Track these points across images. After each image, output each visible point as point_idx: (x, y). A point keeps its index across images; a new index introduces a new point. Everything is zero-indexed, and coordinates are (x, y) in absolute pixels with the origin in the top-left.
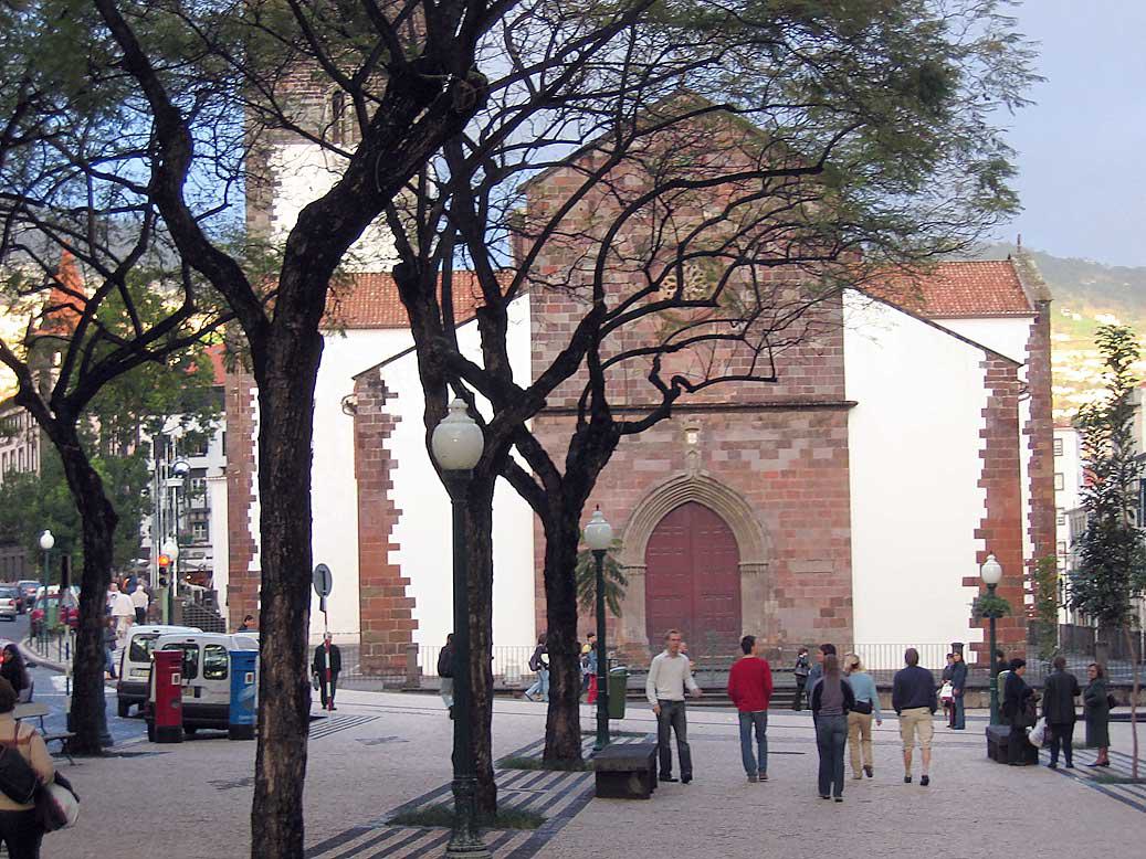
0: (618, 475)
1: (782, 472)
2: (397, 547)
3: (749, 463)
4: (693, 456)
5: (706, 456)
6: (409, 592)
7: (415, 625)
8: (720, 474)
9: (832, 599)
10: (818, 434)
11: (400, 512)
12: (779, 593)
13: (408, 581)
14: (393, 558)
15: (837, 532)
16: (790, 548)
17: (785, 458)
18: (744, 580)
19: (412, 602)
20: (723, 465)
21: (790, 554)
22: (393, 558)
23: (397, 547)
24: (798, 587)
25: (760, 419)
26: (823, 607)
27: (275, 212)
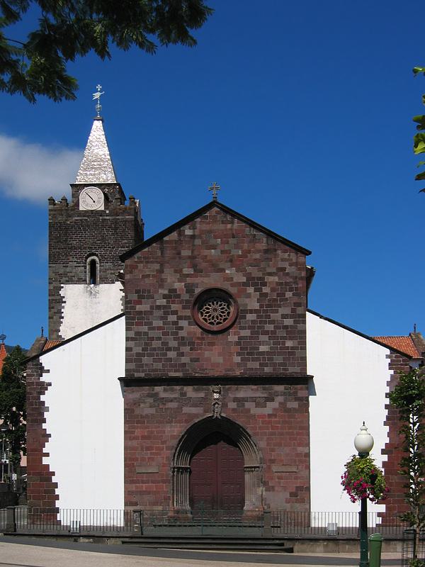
0: (174, 416)
1: (268, 414)
2: (47, 455)
3: (249, 410)
5: (225, 405)
6: (54, 479)
7: (57, 497)
8: (232, 417)
9: (297, 487)
10: (290, 394)
11: (50, 435)
12: (265, 484)
13: (53, 474)
14: (45, 461)
15: (300, 449)
17: (270, 407)
18: (247, 476)
19: (56, 485)
20: (233, 409)
21: (273, 461)
22: (45, 461)
23: (47, 455)
24: (277, 480)
26: (291, 491)
27: (63, 315)
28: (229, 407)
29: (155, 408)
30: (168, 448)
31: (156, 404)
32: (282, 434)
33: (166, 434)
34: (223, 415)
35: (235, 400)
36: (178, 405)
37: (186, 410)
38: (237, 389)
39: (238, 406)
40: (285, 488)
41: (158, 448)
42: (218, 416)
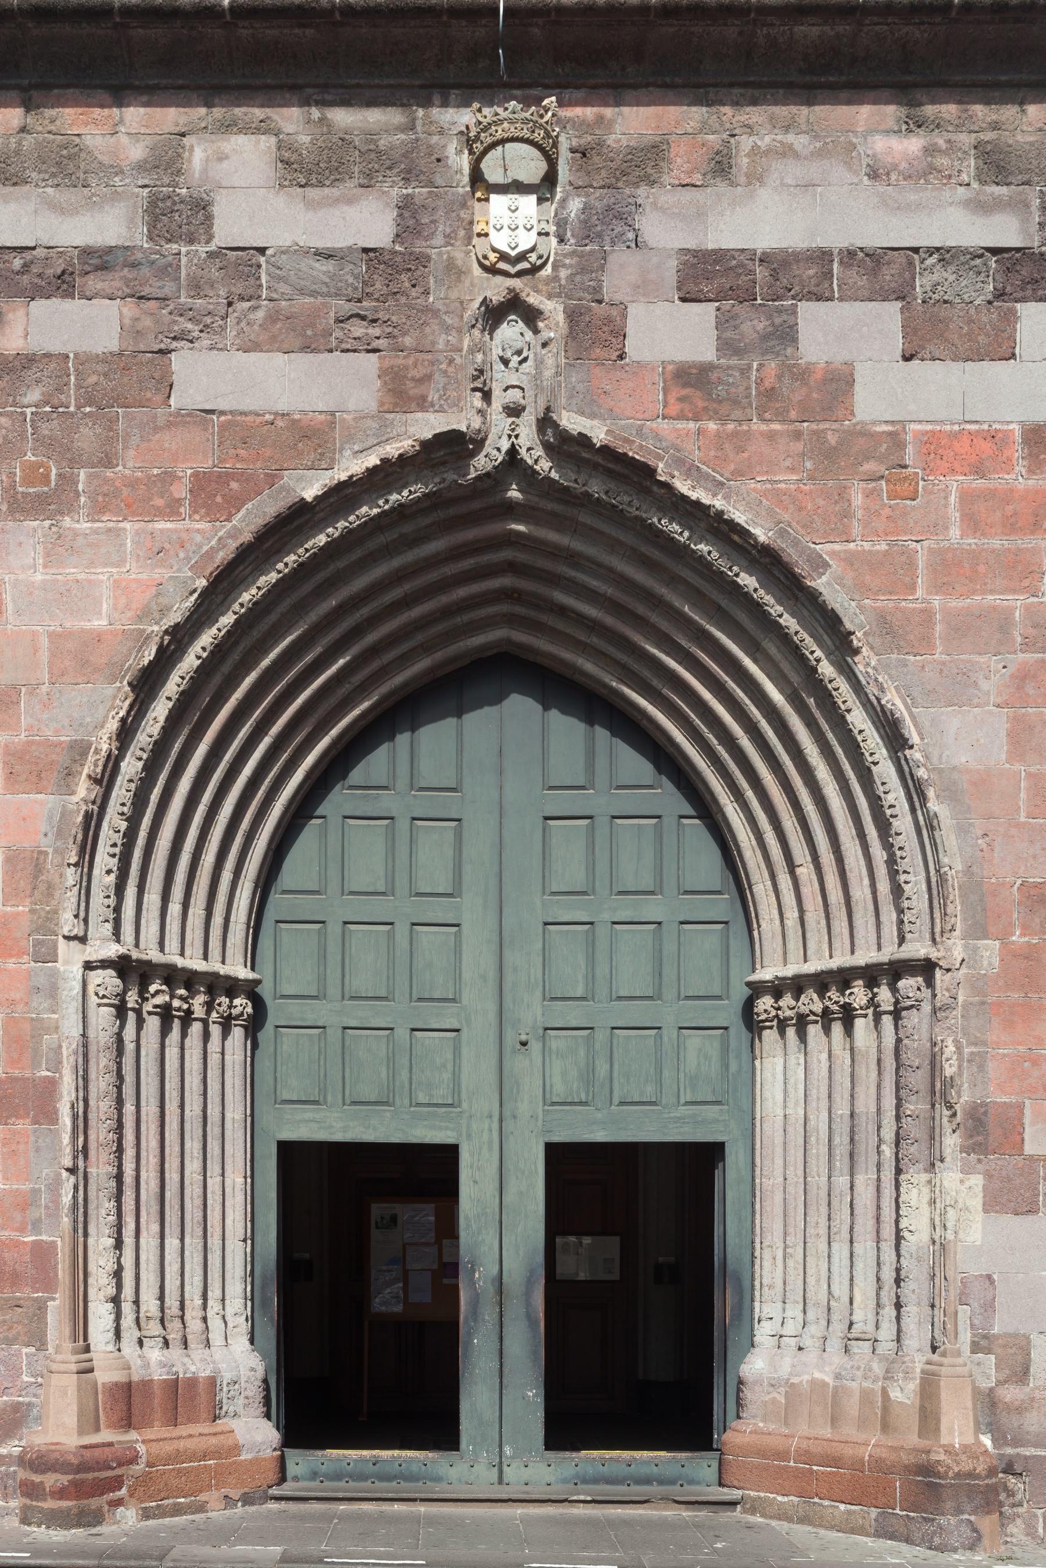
5: (596, 332)
36: (131, 331)
38: (721, 166)
39: (726, 346)
42: (527, 436)
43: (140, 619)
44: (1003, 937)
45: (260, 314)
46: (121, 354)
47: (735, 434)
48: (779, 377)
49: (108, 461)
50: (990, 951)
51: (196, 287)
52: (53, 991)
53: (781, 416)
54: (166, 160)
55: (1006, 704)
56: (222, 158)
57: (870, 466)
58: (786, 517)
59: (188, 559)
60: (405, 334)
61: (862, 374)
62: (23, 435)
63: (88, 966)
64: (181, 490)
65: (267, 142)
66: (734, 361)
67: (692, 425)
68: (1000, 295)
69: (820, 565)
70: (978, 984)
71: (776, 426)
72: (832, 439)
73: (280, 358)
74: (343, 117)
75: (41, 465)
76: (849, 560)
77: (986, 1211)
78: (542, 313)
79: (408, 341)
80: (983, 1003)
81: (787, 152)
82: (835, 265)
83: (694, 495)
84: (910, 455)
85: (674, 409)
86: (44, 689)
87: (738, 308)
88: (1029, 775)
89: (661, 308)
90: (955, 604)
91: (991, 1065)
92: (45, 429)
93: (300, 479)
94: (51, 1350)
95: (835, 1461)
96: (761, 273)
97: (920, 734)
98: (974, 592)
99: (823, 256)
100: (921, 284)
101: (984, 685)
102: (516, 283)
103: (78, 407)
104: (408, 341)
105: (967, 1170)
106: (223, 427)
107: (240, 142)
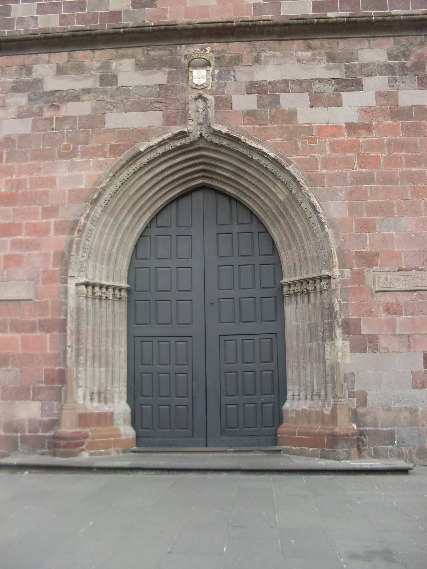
0: (82, 136)
3: (292, 115)
4: (201, 104)
5: (224, 103)
10: (403, 69)
12: (350, 328)
16: (368, 249)
17: (353, 105)
20: (250, 114)
21: (369, 259)
24: (384, 316)
25: (309, 48)
28: (236, 106)
29: (30, 121)
30: (60, 228)
31: (35, 108)
32: (389, 179)
33: (59, 187)
34: (217, 127)
35: (253, 88)
36: (94, 109)
37: (116, 119)
38: (257, 60)
39: (260, 105)
40: (408, 341)
41: (34, 230)
43: (94, 185)
44: (351, 268)
45: (130, 103)
46: (91, 115)
47: (264, 128)
48: (276, 113)
49: (87, 143)
50: (347, 271)
51: (112, 96)
52: (66, 292)
53: (277, 123)
54: (106, 65)
55: (347, 200)
56: (120, 65)
57: (303, 135)
58: (280, 150)
59: (108, 168)
60: (170, 105)
61: (299, 111)
62: (63, 138)
63: (77, 285)
64: (107, 150)
65: (132, 60)
66: (262, 109)
67: (251, 126)
68: (336, 90)
69: (290, 163)
70: (344, 282)
71: (276, 126)
72: (292, 128)
73: (135, 113)
74: (153, 53)
75: (68, 145)
76: (299, 161)
77: (351, 351)
78: (207, 99)
79: (171, 107)
80: (346, 288)
81: (275, 56)
82: (290, 84)
83: (252, 145)
84: (314, 132)
85: (246, 122)
86: (66, 205)
87: (263, 95)
88: (355, 220)
89: (241, 96)
90: (331, 172)
91: (350, 307)
92: (70, 135)
93: (140, 145)
94: (63, 402)
95: (308, 434)
96: (269, 86)
97: (322, 209)
98: (335, 169)
99: (287, 81)
100: (314, 89)
101: (340, 195)
102: (201, 92)
103: (79, 129)
104: (171, 107)
105: (344, 340)
106: (119, 132)
107: (125, 60)
